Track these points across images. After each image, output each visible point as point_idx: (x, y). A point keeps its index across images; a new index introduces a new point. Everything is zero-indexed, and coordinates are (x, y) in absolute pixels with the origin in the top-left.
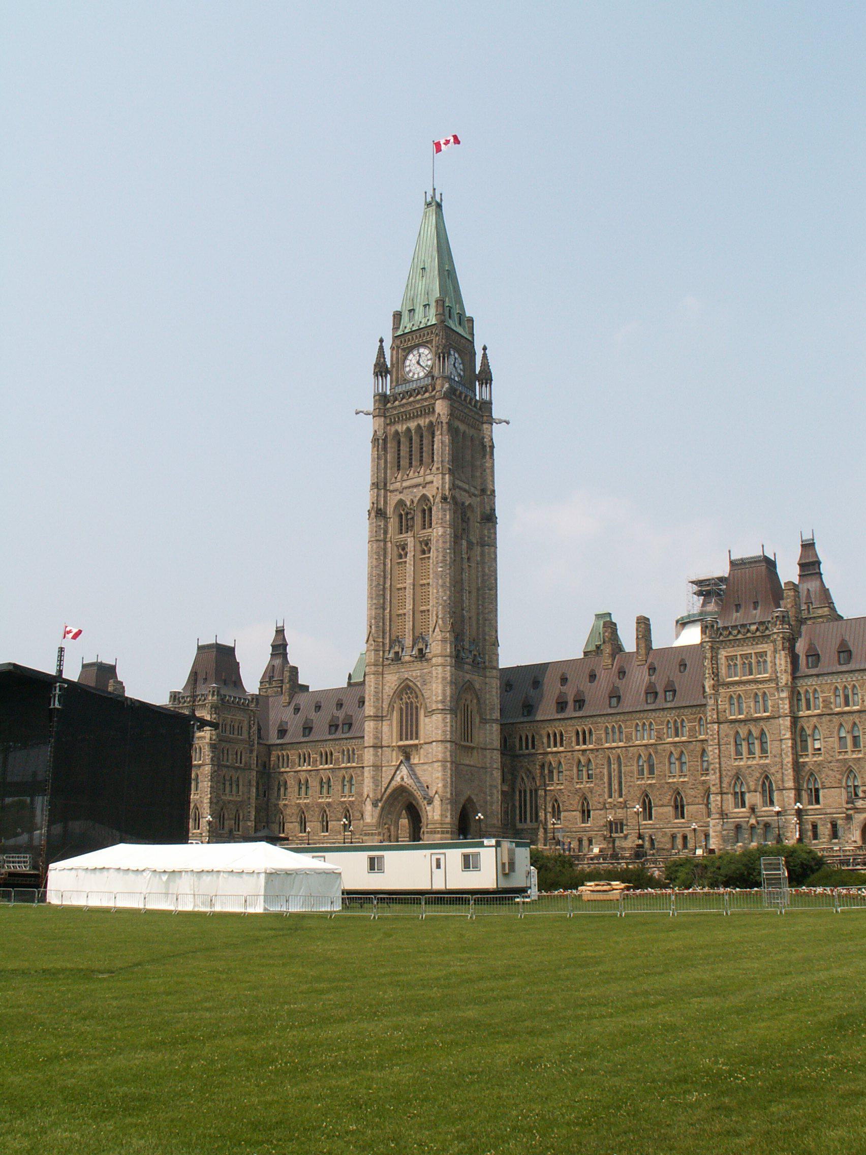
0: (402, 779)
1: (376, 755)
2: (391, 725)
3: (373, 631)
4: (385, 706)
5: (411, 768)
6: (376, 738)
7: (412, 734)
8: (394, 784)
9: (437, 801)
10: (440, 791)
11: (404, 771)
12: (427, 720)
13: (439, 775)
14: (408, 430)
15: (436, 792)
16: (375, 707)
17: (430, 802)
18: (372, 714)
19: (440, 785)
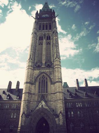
0: (42, 106)
1: (29, 97)
2: (35, 86)
3: (32, 57)
4: (33, 80)
5: (46, 102)
6: (29, 90)
7: (44, 91)
8: (38, 108)
9: (61, 117)
10: (62, 112)
11: (43, 103)
12: (52, 86)
13: (62, 105)
14: (44, 24)
15: (61, 112)
16: (30, 79)
17: (58, 116)
18: (28, 81)
19: (62, 109)
